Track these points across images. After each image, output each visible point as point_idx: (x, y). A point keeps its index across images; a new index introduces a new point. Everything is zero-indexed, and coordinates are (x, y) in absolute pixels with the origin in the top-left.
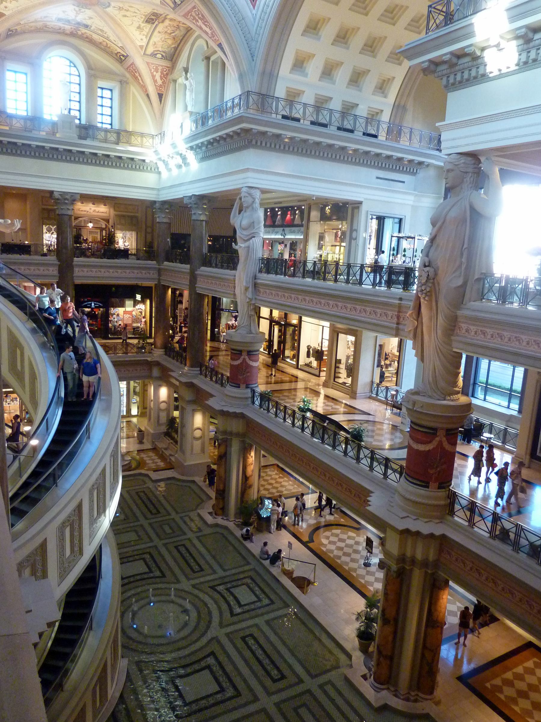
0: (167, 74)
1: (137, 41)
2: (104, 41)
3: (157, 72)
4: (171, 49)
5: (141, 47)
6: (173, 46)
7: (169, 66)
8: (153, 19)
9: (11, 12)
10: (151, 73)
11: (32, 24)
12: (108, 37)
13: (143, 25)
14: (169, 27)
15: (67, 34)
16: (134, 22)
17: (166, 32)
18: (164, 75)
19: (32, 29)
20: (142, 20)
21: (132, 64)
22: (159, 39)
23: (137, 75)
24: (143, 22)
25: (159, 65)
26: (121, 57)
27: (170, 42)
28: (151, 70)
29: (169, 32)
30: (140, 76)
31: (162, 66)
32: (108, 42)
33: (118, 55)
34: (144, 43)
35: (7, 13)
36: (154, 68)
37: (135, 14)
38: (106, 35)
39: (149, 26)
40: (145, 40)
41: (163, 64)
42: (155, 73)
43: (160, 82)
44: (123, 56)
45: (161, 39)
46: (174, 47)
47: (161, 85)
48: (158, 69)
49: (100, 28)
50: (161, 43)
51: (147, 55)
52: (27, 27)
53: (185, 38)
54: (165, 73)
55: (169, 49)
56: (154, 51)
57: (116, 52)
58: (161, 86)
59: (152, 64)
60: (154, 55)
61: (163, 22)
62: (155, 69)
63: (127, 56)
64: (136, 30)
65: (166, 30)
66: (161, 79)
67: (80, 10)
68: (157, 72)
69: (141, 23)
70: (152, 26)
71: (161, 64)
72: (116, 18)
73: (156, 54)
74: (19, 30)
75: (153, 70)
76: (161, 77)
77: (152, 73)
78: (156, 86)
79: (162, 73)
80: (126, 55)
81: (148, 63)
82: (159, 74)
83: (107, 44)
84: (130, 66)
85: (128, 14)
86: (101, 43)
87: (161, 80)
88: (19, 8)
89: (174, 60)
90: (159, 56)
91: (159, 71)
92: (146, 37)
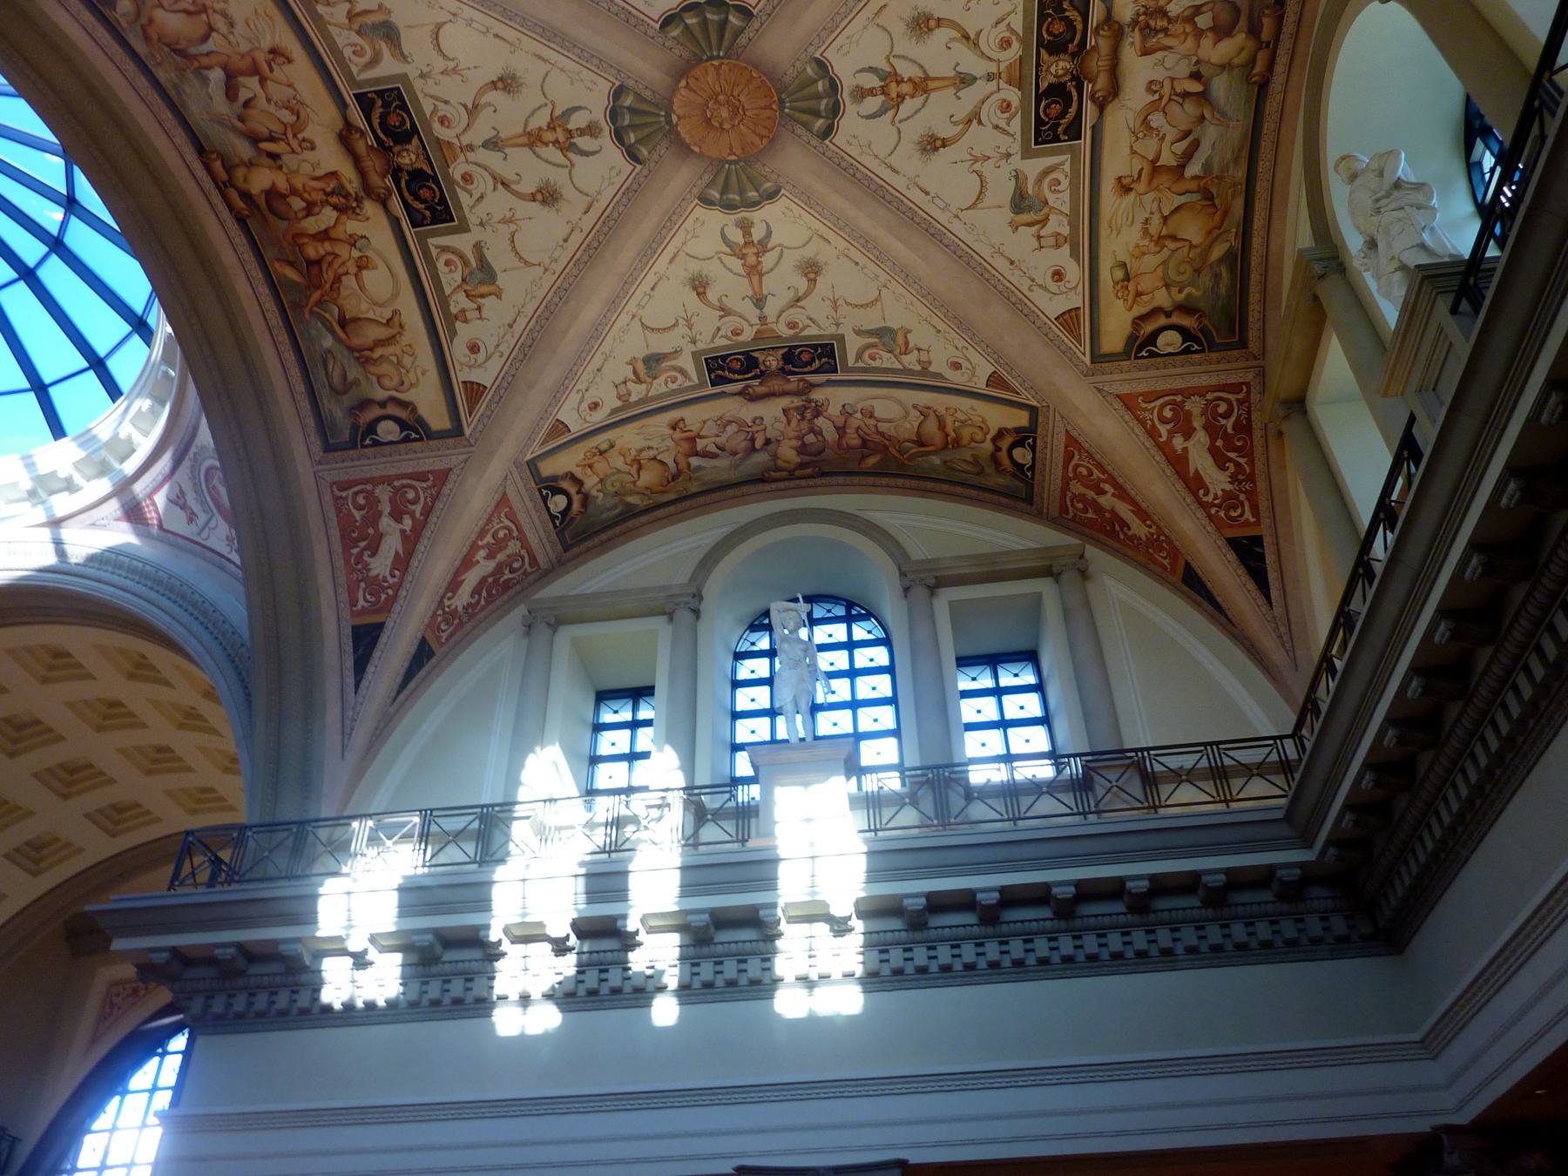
0: (1244, 428)
1: (1039, 297)
2: (925, 412)
3: (1188, 433)
4: (1217, 277)
5: (1068, 319)
6: (1218, 252)
7: (1234, 379)
8: (1057, 92)
9: (496, 364)
10: (1159, 446)
11: (630, 438)
12: (924, 371)
13: (1033, 167)
14: (1157, 120)
15: (791, 475)
16: (987, 168)
17: (1156, 169)
18: (1226, 437)
19: (648, 477)
20: (1016, 125)
21: (1069, 457)
22: (1133, 236)
23: (1107, 501)
24: (1027, 154)
25: (1188, 393)
26: (1018, 454)
27: (1193, 229)
28: (1153, 433)
29: (1167, 159)
30: (1122, 494)
31: (1200, 392)
32: (939, 401)
33: (1003, 455)
34: (1077, 300)
35: (485, 377)
36: (1168, 413)
37: (971, 96)
38: (910, 361)
39: (1058, 160)
40: (1075, 273)
41: (1205, 380)
42: (1178, 442)
43: (1218, 481)
44: (1024, 437)
45: (1146, 232)
46: (1229, 258)
47: (1228, 495)
48: (1188, 415)
49: (872, 320)
50: (1152, 261)
51: (1112, 357)
52: (618, 462)
53: (1264, 166)
54: (1229, 424)
55: (1206, 279)
56: (1139, 321)
57: (988, 446)
58: (1229, 499)
59: (1151, 396)
60: (1141, 345)
61: (1115, 90)
62: (1175, 419)
63: (1033, 411)
64: (1015, 227)
65: (1148, 147)
66: (1220, 461)
67: (745, 227)
68: (1188, 433)
69: (1017, 162)
70: (1075, 161)
71: (1195, 382)
72: (899, 182)
73: (1152, 339)
74: (590, 482)
75: (1163, 430)
76: (1213, 451)
77: (1165, 449)
78: (1204, 506)
79: (1212, 430)
80: (1021, 419)
81: (1128, 402)
82: (1201, 437)
83: (942, 425)
84: (1066, 482)
85: (938, 113)
86: (920, 441)
87: (1223, 468)
88: (518, 327)
89: (1253, 335)
90: (1169, 341)
91: (1198, 422)
92: (1075, 253)
